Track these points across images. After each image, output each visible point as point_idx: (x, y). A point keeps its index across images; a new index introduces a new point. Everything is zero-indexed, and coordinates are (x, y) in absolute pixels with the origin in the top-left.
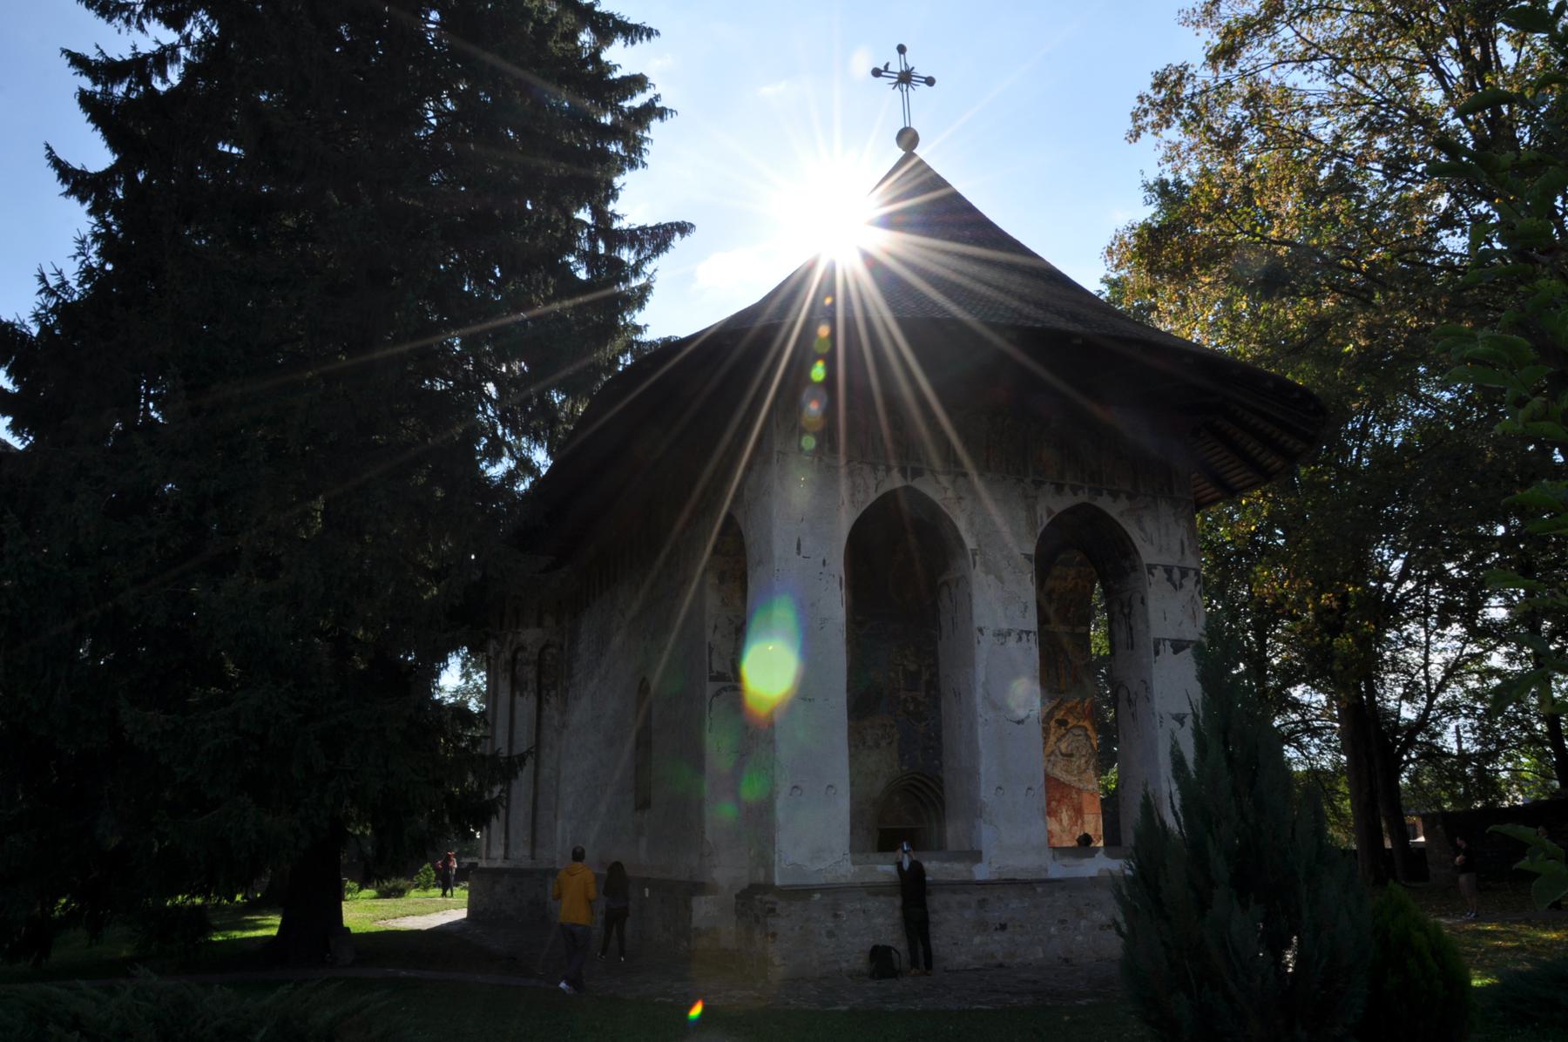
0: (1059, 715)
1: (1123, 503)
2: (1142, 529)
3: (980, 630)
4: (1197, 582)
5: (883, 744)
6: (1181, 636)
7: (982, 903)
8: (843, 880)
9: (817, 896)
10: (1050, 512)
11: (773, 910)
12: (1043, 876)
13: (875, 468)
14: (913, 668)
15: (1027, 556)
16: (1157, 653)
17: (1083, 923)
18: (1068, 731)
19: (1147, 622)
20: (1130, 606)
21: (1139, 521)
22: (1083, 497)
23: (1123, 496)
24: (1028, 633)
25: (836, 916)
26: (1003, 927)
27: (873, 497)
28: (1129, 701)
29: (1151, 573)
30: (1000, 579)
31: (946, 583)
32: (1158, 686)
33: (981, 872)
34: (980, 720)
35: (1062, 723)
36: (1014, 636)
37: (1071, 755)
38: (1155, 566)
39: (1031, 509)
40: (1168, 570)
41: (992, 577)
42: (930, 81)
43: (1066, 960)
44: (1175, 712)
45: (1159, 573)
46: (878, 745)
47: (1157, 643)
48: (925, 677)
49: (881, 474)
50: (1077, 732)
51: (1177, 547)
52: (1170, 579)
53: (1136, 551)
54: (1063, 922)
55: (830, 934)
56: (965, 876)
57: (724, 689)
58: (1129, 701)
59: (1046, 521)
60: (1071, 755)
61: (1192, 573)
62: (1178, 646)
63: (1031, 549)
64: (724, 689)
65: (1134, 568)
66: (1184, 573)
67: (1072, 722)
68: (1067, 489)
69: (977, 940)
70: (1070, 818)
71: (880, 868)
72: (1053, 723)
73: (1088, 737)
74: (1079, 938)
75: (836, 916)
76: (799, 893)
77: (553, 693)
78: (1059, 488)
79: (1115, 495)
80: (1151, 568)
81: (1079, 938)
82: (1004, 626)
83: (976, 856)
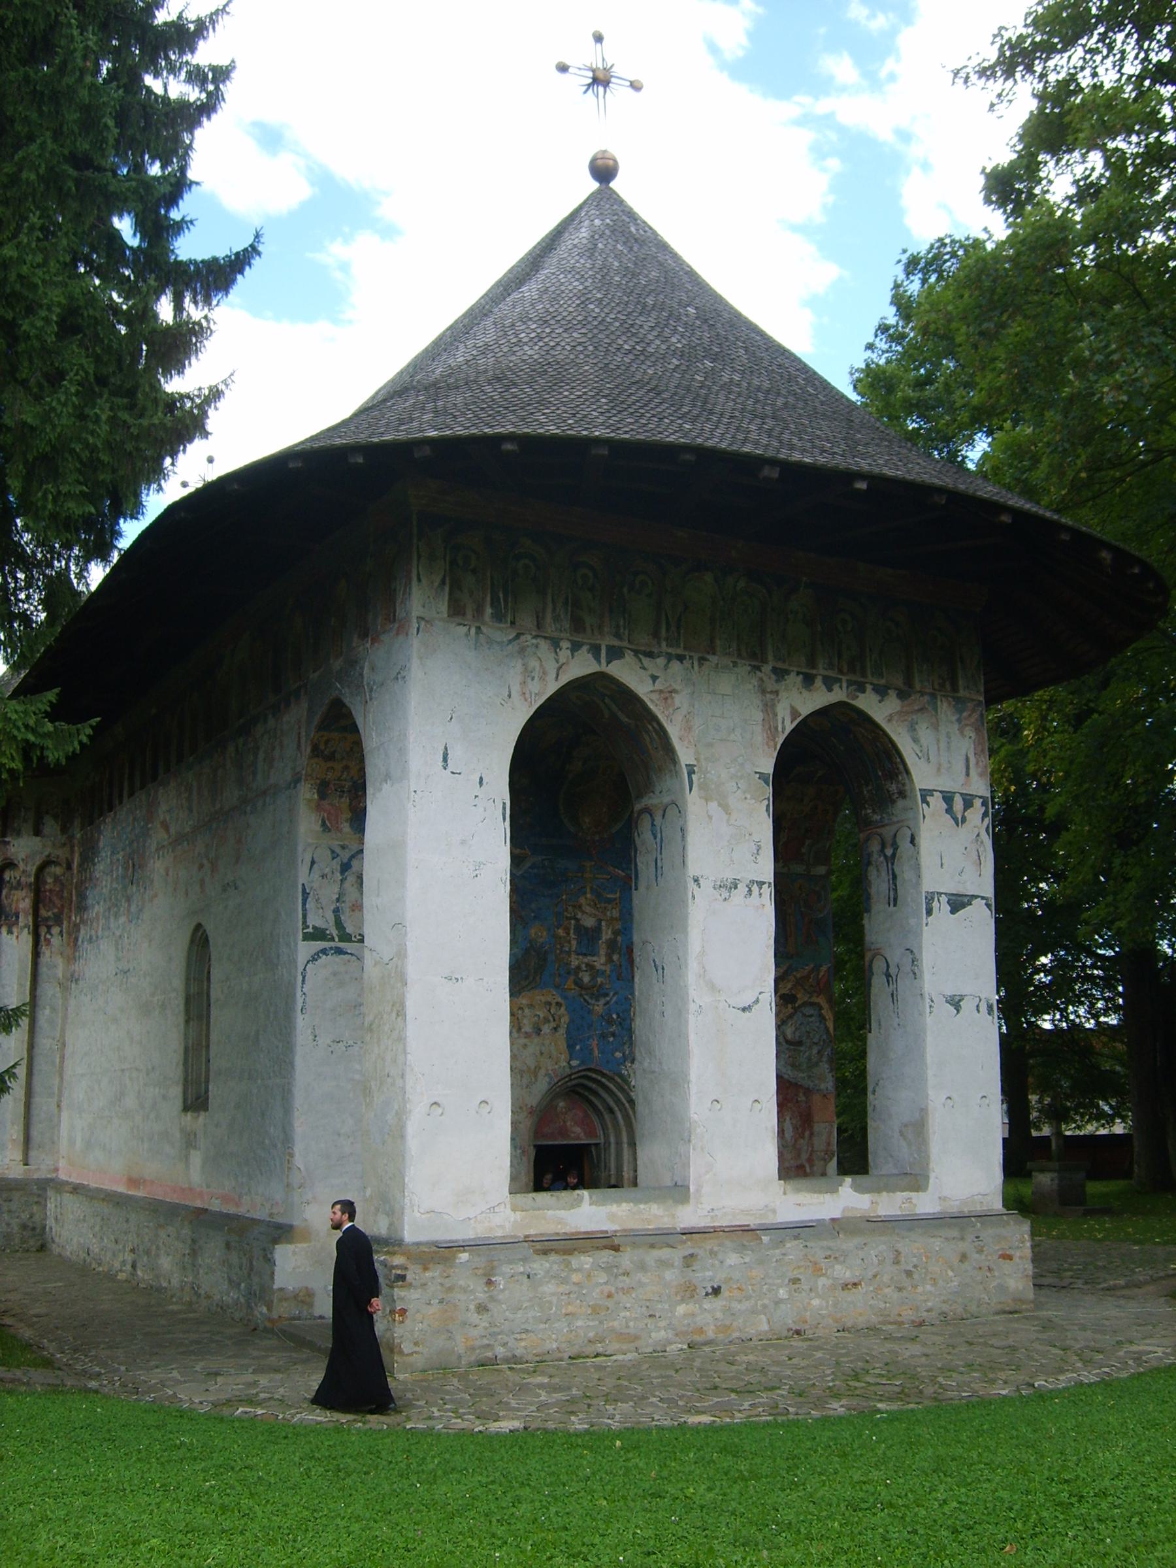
1: (892, 704)
2: (916, 740)
3: (696, 880)
4: (985, 815)
5: (546, 1029)
6: (962, 891)
7: (689, 1260)
8: (500, 1233)
9: (464, 1256)
10: (794, 713)
11: (402, 1278)
12: (770, 1220)
13: (555, 644)
14: (589, 922)
15: (763, 776)
16: (929, 912)
17: (822, 1281)
18: (796, 1009)
19: (917, 868)
20: (895, 847)
21: (912, 728)
22: (839, 695)
23: (892, 694)
24: (761, 884)
25: (489, 1283)
26: (716, 1291)
27: (552, 688)
28: (888, 975)
29: (924, 801)
30: (726, 808)
31: (647, 810)
32: (927, 959)
33: (688, 1216)
34: (692, 1007)
36: (742, 888)
37: (800, 1043)
38: (930, 792)
39: (769, 709)
40: (948, 798)
41: (713, 805)
42: (635, 86)
43: (798, 1332)
44: (949, 992)
45: (936, 802)
46: (538, 1031)
47: (930, 898)
48: (607, 934)
49: (564, 654)
50: (808, 1011)
51: (960, 766)
52: (949, 810)
53: (908, 772)
54: (795, 1281)
55: (482, 1308)
56: (666, 1223)
57: (324, 951)
58: (888, 975)
59: (790, 727)
60: (800, 1043)
61: (978, 803)
62: (958, 903)
63: (768, 767)
64: (324, 951)
65: (902, 794)
66: (968, 803)
67: (802, 997)
68: (819, 682)
69: (681, 1309)
70: (795, 1128)
73: (822, 1018)
74: (816, 1302)
75: (489, 1283)
76: (441, 1253)
77: (55, 930)
78: (808, 680)
79: (882, 692)
80: (926, 794)
81: (816, 1302)
82: (729, 875)
83: (679, 1192)
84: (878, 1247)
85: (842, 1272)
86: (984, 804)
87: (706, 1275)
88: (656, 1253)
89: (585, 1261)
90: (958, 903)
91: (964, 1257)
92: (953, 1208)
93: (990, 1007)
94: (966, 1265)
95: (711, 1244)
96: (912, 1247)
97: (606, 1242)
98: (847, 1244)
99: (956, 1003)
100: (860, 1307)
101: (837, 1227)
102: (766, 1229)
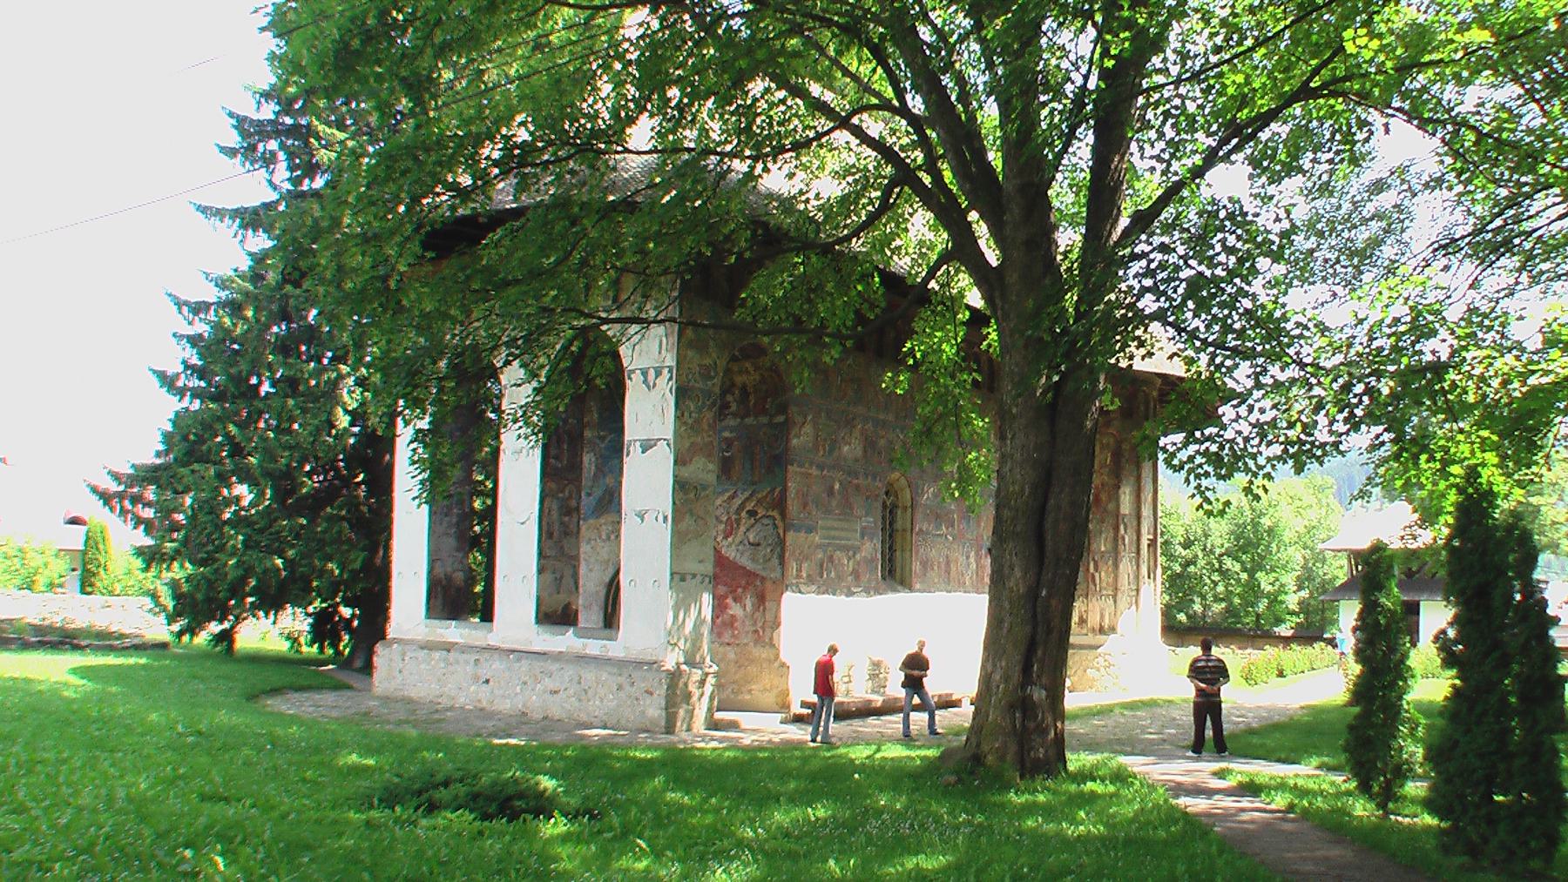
0: (749, 507)
35: (752, 513)
40: (645, 373)
46: (609, 538)
50: (766, 521)
52: (645, 381)
66: (658, 373)
67: (761, 512)
71: (440, 631)
72: (744, 514)
80: (633, 371)
84: (570, 671)
85: (549, 683)
86: (670, 371)
87: (484, 672)
88: (465, 656)
89: (437, 655)
90: (647, 446)
91: (620, 688)
92: (634, 655)
93: (665, 518)
94: (621, 694)
95: (487, 655)
96: (589, 675)
97: (448, 647)
98: (554, 667)
99: (641, 516)
100: (558, 708)
101: (558, 657)
102: (513, 651)
